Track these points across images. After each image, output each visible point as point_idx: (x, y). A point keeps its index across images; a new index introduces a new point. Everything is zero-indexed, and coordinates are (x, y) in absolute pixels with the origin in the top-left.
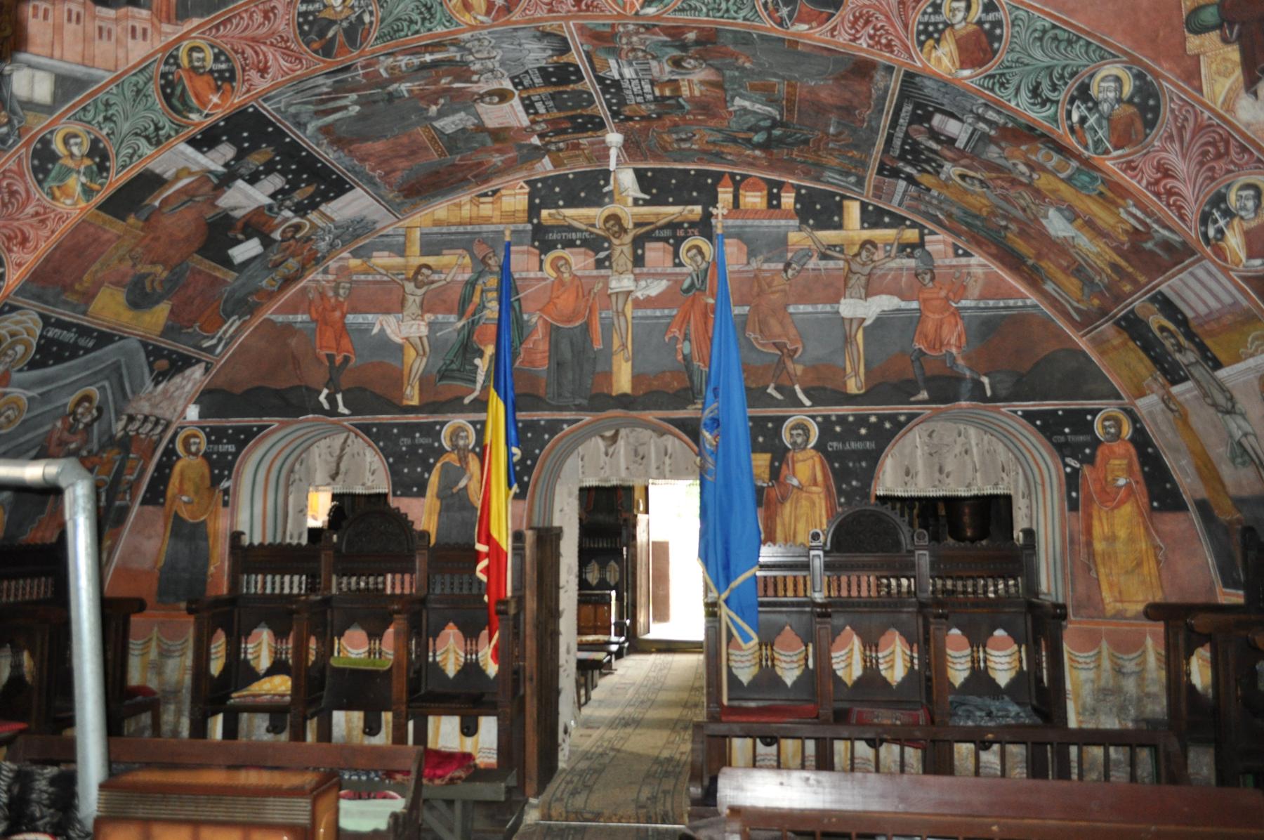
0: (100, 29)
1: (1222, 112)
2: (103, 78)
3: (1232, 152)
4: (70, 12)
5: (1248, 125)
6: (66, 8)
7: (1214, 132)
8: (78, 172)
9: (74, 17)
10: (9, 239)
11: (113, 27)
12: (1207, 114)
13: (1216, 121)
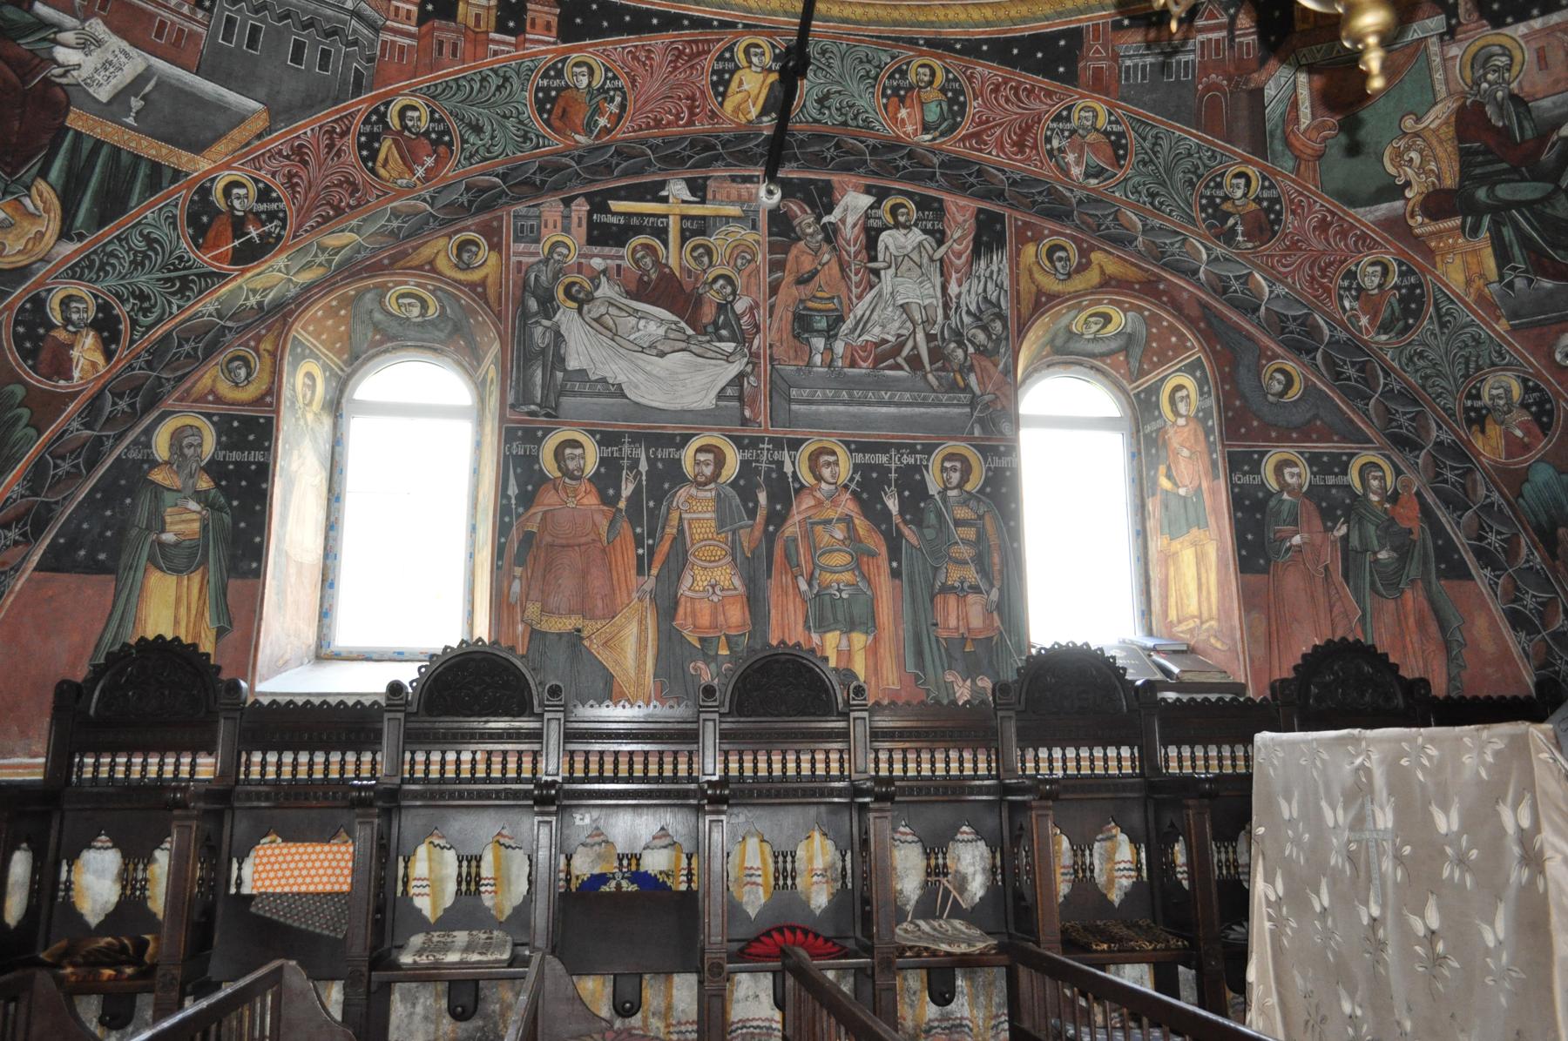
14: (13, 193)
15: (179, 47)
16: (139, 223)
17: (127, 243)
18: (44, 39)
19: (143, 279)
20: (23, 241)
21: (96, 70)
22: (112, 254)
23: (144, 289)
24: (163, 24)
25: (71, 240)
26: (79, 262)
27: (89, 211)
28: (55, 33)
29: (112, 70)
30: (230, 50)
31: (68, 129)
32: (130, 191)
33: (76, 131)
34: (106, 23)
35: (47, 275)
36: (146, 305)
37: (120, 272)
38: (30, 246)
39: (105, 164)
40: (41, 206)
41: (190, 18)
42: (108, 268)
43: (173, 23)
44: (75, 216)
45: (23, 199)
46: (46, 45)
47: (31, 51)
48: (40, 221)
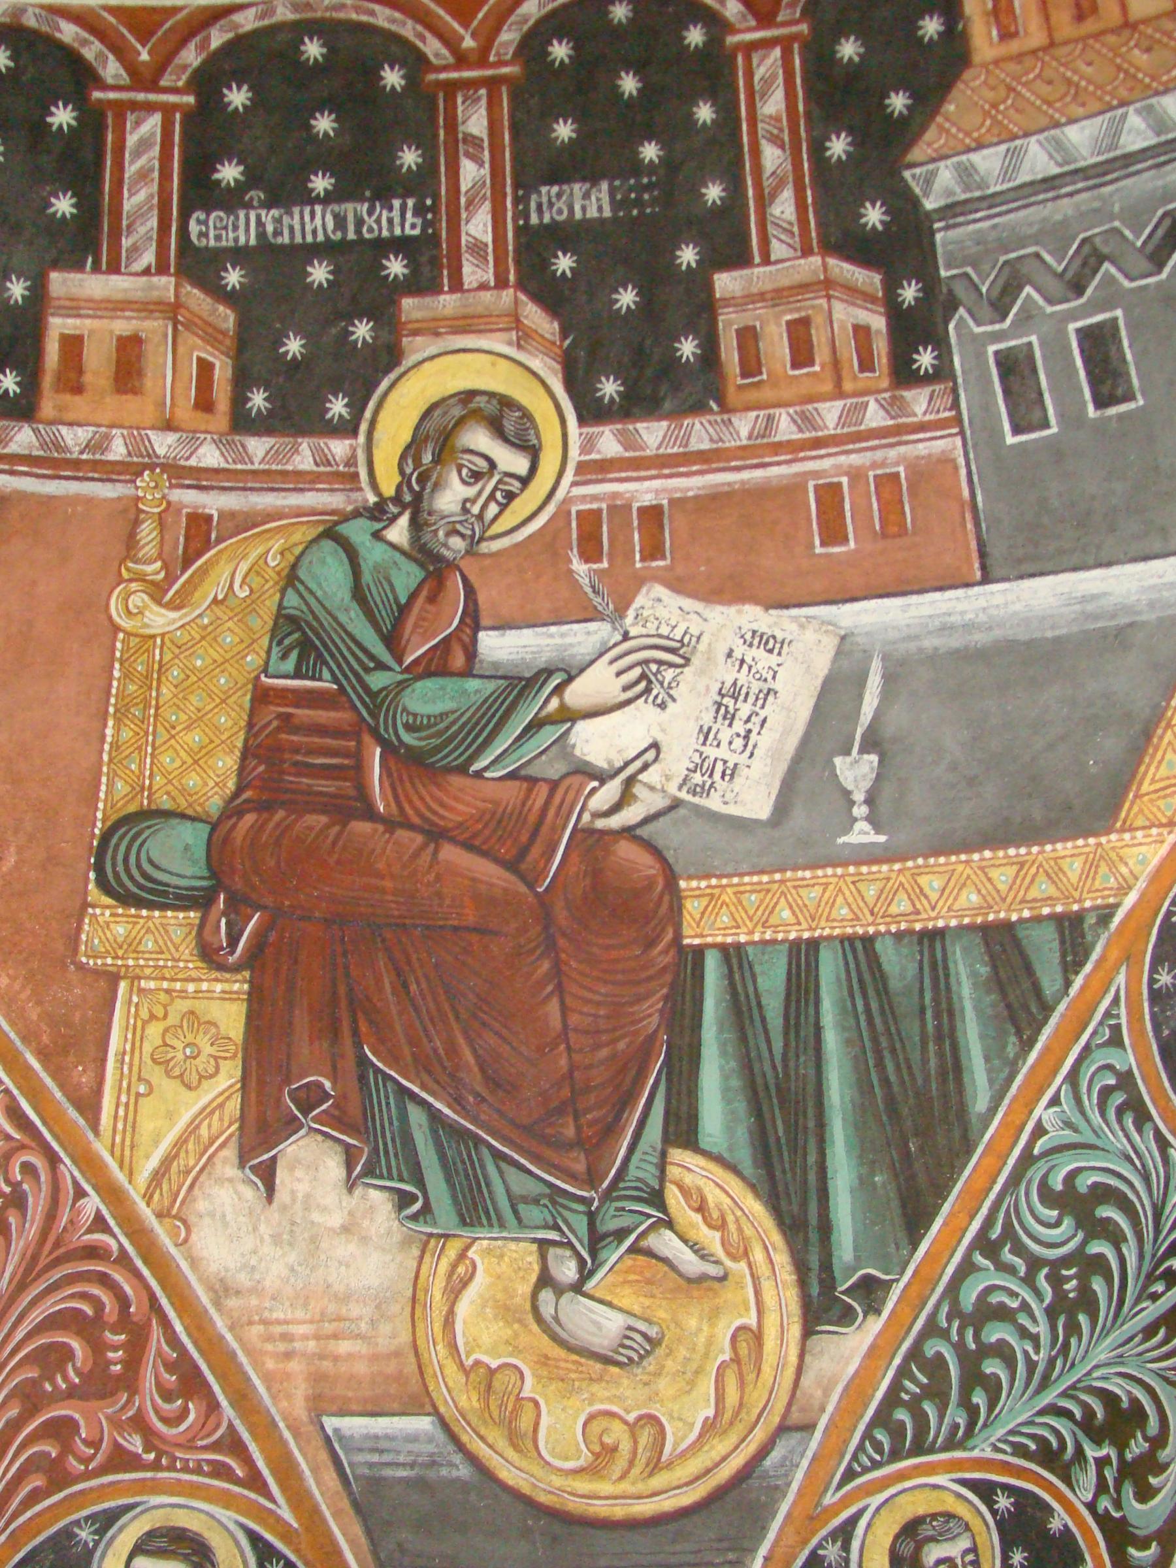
1: (146, 1213)
3: (148, 1381)
5: (222, 1290)
7: (104, 1280)
12: (93, 1203)
13: (116, 1240)
14: (621, 1234)
15: (903, 532)
16: (1027, 1159)
17: (1019, 1249)
18: (536, 725)
19: (1102, 1353)
20: (707, 1386)
21: (705, 734)
22: (987, 1312)
23: (1116, 1387)
24: (830, 495)
25: (846, 1316)
26: (896, 1387)
27: (864, 1184)
28: (559, 690)
29: (745, 709)
30: (1055, 450)
31: (699, 952)
32: (953, 1069)
33: (723, 948)
34: (678, 586)
35: (815, 1483)
36: (1137, 1447)
37: (1031, 1366)
38: (732, 1396)
39: (847, 1011)
40: (712, 1239)
41: (898, 430)
42: (992, 1367)
43: (856, 475)
44: (826, 1228)
45: (652, 1241)
46: (548, 735)
47: (512, 776)
48: (728, 1294)
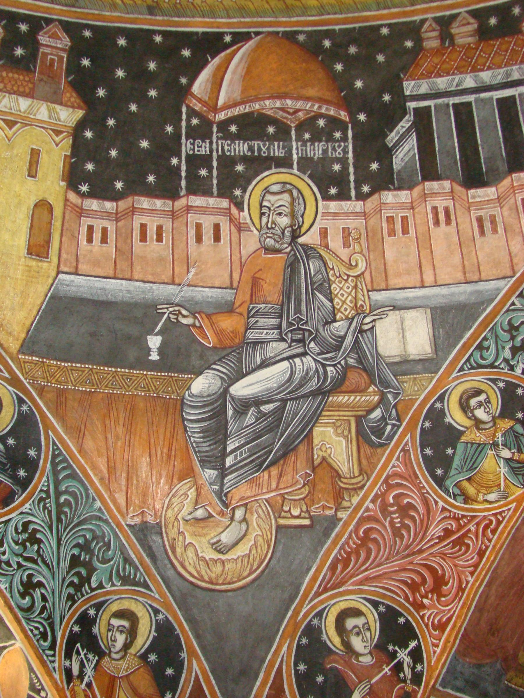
0: (480, 220)
2: (499, 290)
4: (435, 209)
6: (429, 208)
8: (495, 445)
9: (442, 217)
10: (414, 587)
11: (497, 211)
